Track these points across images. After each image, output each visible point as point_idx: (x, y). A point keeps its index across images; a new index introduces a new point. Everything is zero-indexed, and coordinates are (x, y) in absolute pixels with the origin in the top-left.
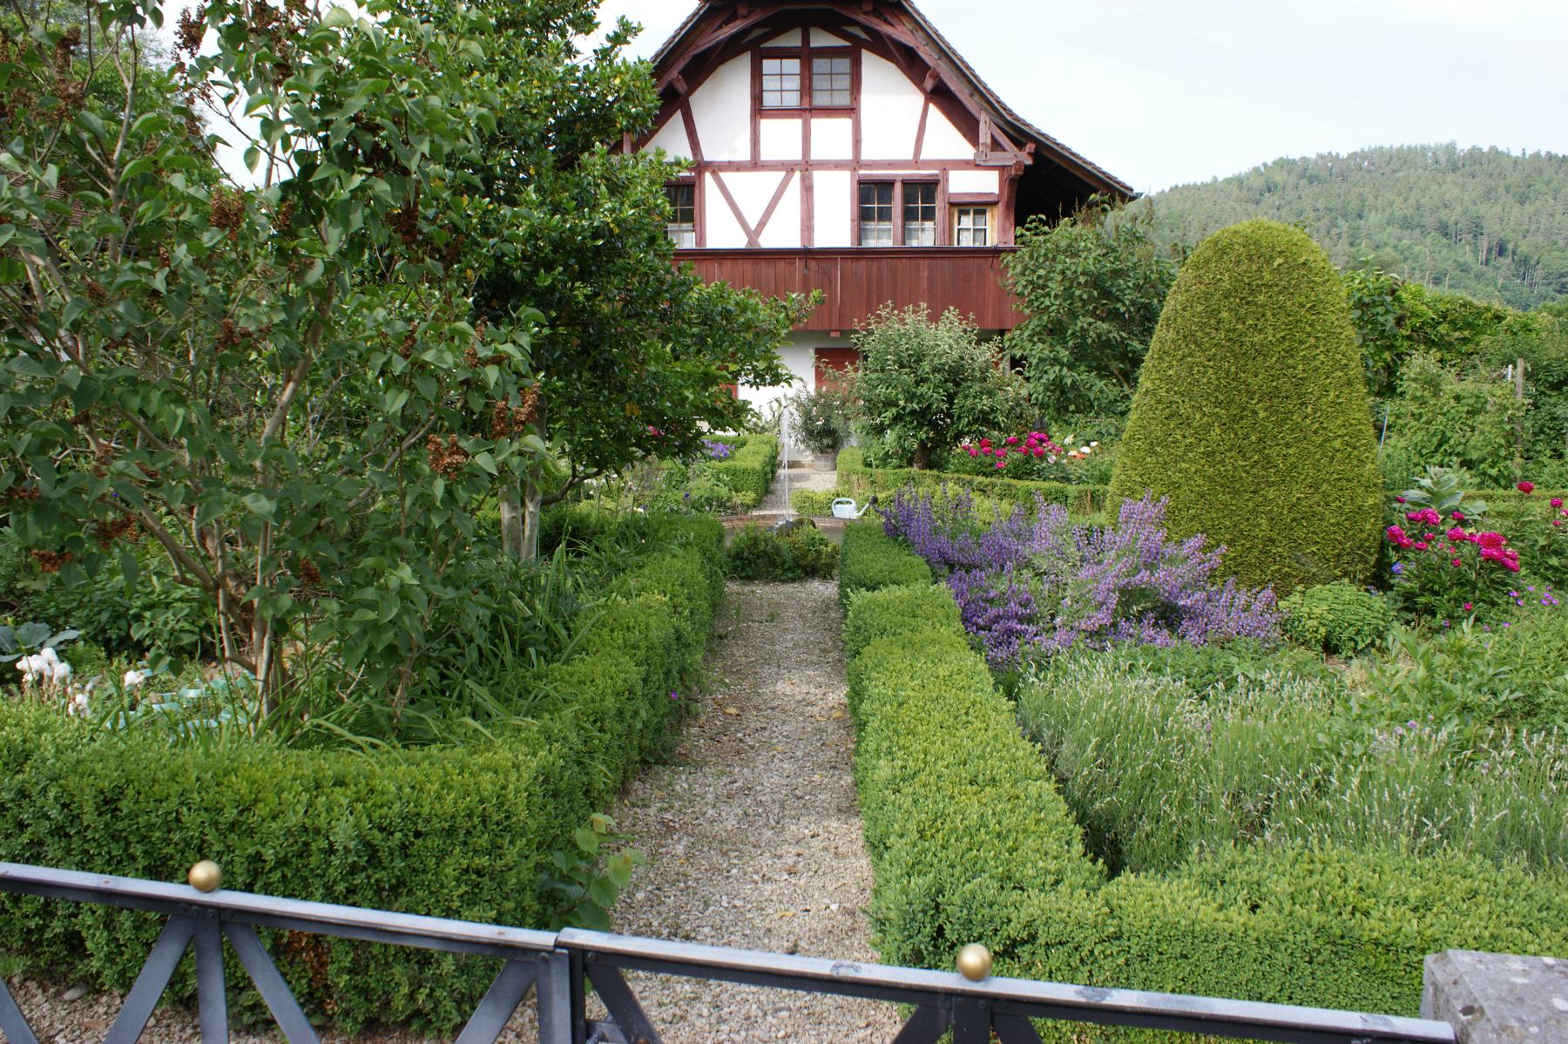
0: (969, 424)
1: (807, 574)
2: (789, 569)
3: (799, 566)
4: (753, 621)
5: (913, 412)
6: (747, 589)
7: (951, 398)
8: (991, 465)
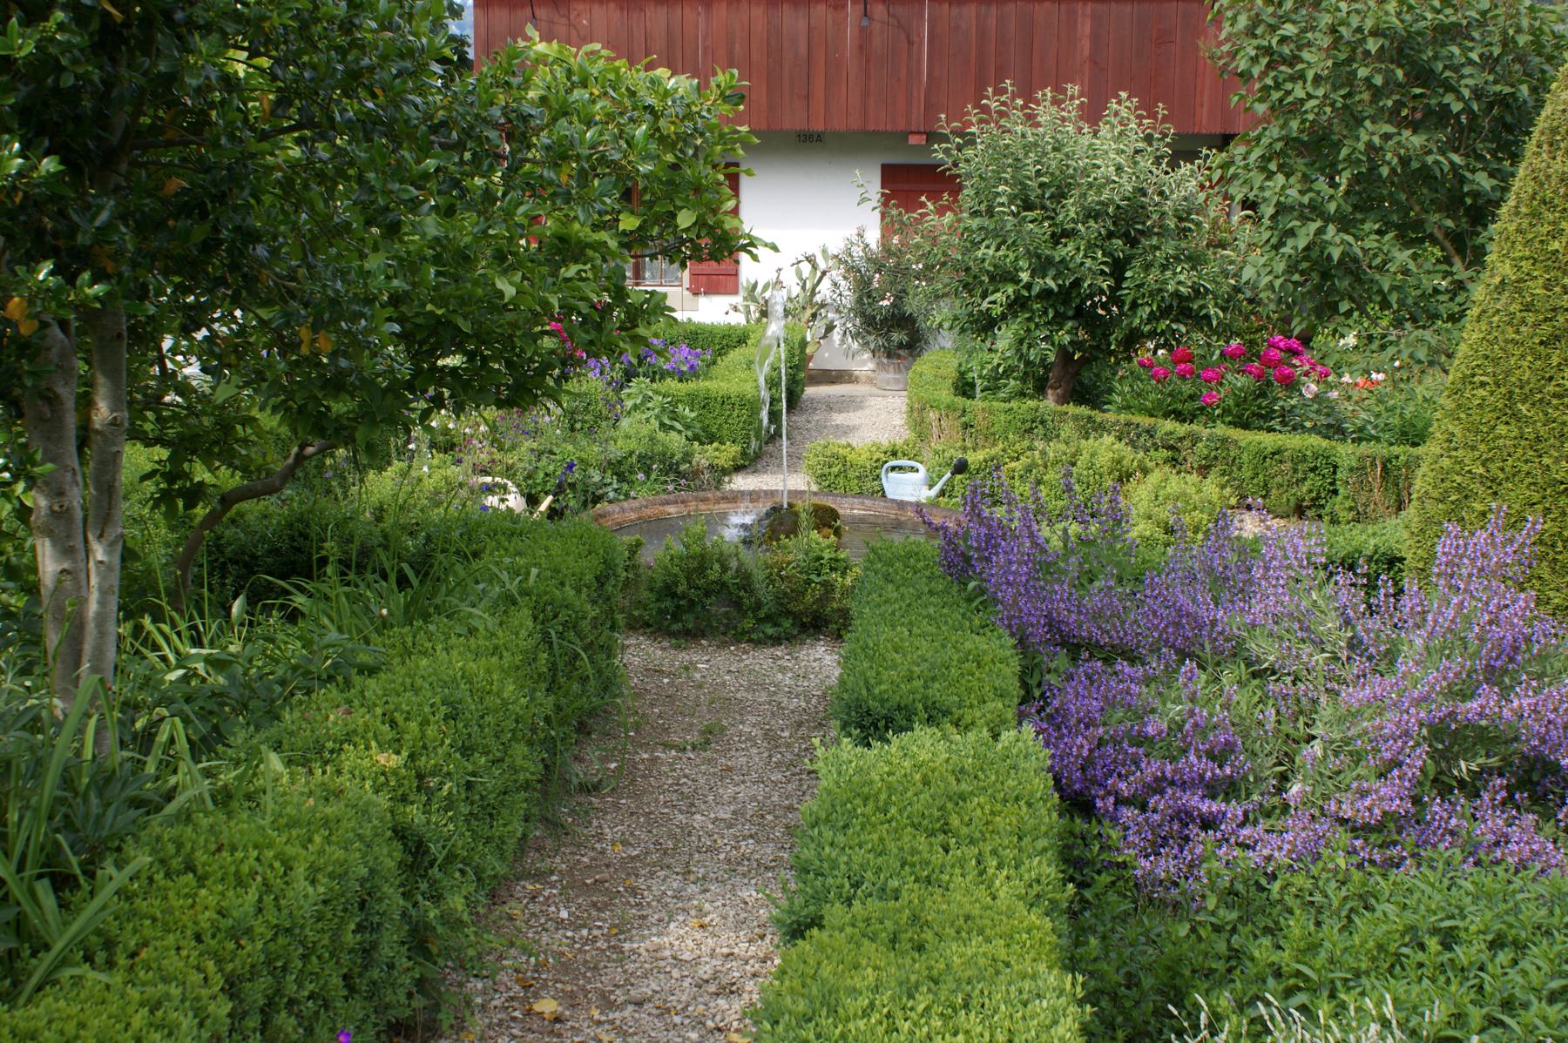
0: (1152, 317)
1: (804, 627)
2: (769, 618)
3: (789, 613)
4: (667, 746)
5: (1046, 294)
6: (684, 657)
7: (1118, 268)
8: (1192, 397)
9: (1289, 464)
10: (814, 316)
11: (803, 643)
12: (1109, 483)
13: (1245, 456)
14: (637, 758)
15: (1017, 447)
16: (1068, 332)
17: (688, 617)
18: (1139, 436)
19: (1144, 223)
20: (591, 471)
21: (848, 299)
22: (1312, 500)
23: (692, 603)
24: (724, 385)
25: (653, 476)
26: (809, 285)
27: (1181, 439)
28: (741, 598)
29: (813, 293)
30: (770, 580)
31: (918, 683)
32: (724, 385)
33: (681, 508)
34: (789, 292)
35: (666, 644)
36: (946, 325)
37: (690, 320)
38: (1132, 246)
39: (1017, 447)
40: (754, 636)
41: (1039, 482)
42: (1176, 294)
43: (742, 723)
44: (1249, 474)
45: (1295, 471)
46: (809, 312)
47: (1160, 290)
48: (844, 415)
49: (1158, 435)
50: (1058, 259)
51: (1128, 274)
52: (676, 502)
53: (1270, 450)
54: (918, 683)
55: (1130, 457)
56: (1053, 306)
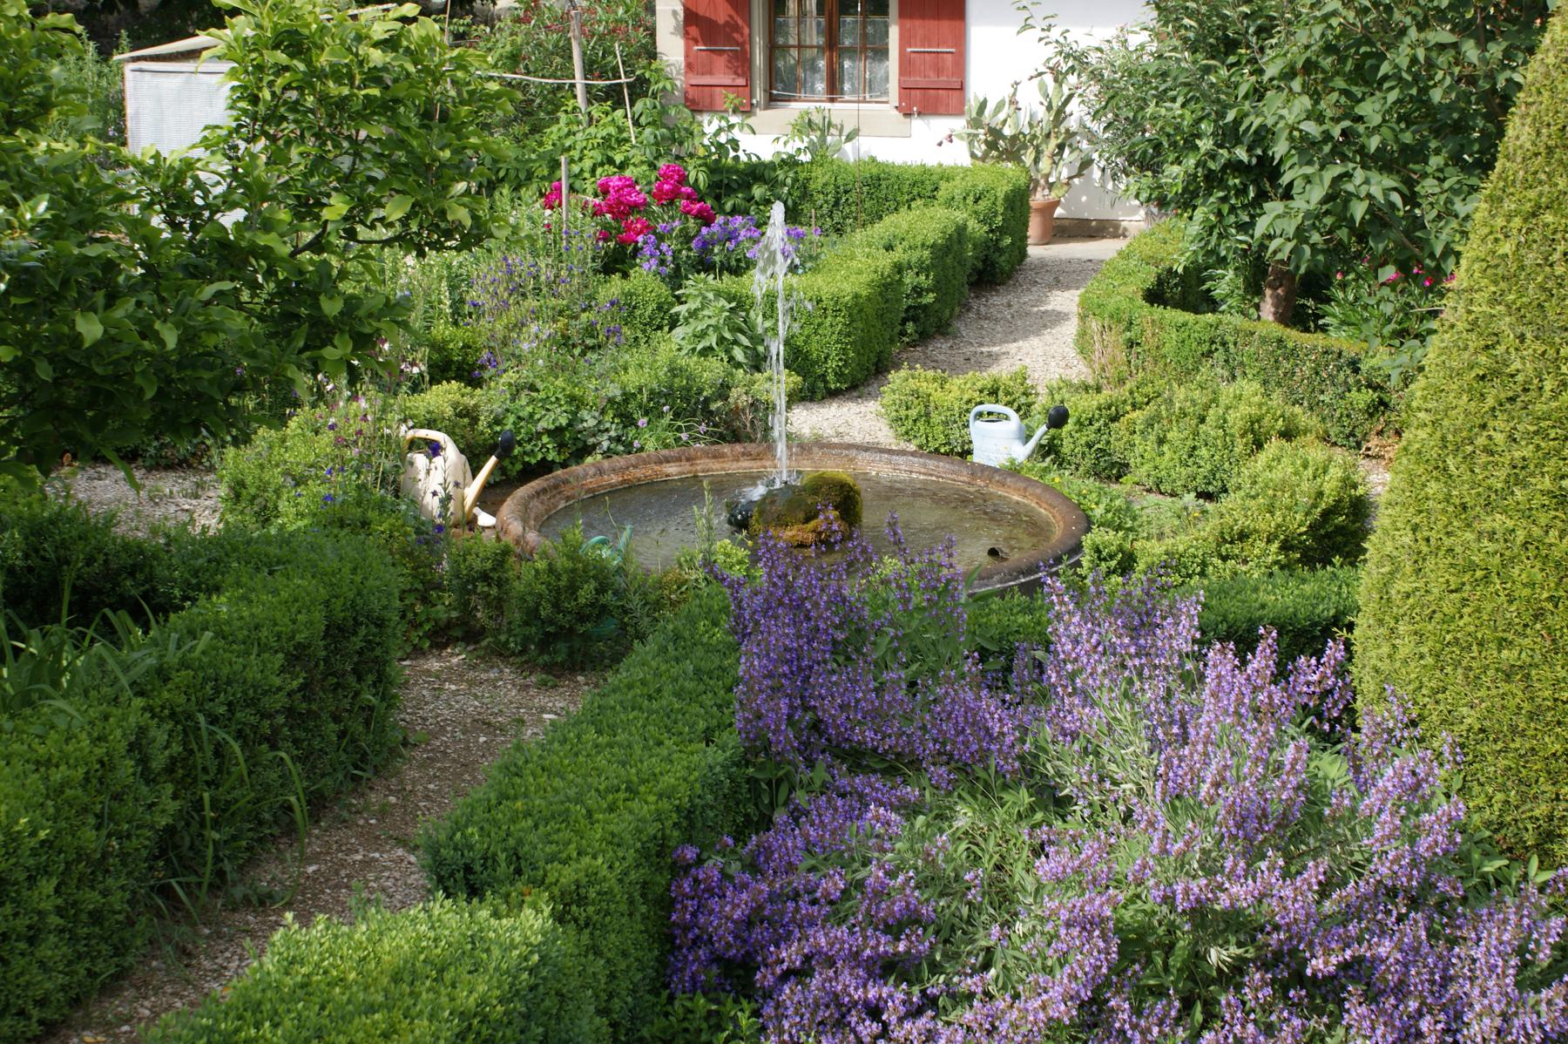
5: (1235, 166)
18: (1340, 369)
20: (584, 414)
33: (686, 467)
41: (1161, 441)
46: (1053, 142)
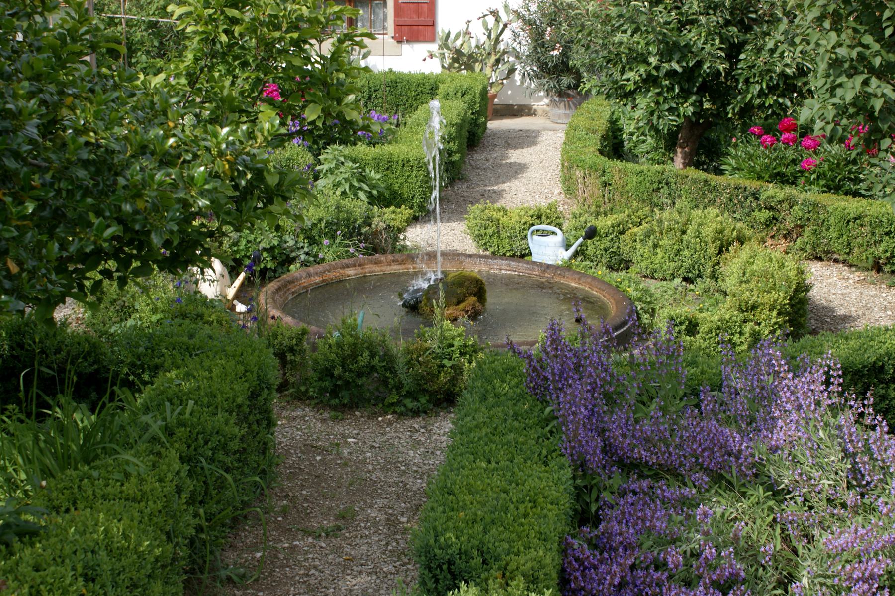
0: (761, 93)
1: (437, 404)
2: (409, 394)
3: (424, 391)
4: (307, 533)
5: (671, 74)
6: (339, 429)
7: (733, 51)
8: (794, 161)
9: (868, 229)
10: (498, 61)
11: (437, 415)
12: (712, 250)
13: (832, 219)
14: (279, 546)
15: (640, 213)
16: (692, 105)
17: (344, 393)
18: (746, 198)
19: (756, 12)
20: (287, 237)
21: (525, 49)
22: (887, 258)
23: (347, 383)
24: (405, 148)
25: (338, 241)
26: (493, 36)
27: (780, 202)
28: (387, 378)
29: (497, 41)
30: (409, 363)
31: (479, 528)
32: (405, 148)
33: (359, 270)
34: (478, 41)
35: (326, 415)
36: (594, 92)
37: (391, 70)
38: (746, 33)
39: (640, 213)
40: (398, 409)
41: (655, 246)
42: (783, 75)
43: (371, 507)
44: (835, 235)
45: (873, 234)
46: (493, 58)
47: (769, 71)
48: (519, 151)
49: (762, 198)
50: (682, 44)
51: (742, 56)
52: (354, 265)
53: (852, 216)
54: (479, 528)
55: (732, 225)
56: (679, 83)
